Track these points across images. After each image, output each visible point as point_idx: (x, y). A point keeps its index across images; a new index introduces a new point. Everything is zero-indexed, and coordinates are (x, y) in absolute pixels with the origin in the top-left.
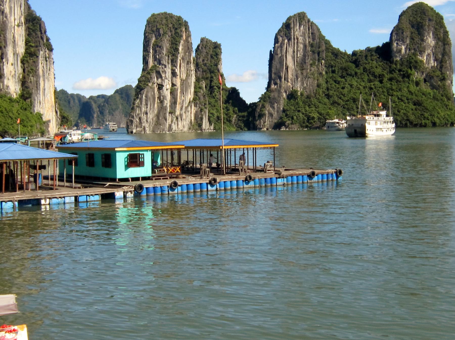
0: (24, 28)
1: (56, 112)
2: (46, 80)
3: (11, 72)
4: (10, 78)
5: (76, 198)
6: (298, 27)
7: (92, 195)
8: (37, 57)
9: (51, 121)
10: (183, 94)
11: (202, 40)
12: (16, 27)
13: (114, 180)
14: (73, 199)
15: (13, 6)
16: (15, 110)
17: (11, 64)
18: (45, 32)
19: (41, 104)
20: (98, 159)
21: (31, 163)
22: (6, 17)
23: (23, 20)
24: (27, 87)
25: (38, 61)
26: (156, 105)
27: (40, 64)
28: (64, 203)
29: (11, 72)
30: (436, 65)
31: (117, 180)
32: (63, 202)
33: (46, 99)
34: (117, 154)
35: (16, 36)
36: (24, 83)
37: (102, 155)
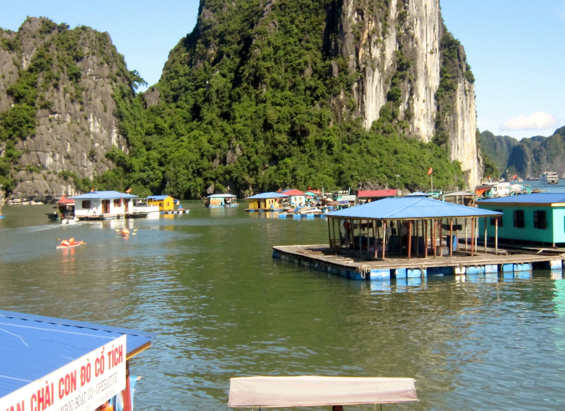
0: (438, 55)
1: (478, 160)
2: (466, 119)
3: (422, 110)
4: (422, 118)
5: (499, 266)
7: (520, 264)
8: (455, 90)
9: (472, 171)
12: (429, 55)
13: (550, 245)
14: (495, 268)
15: (424, 29)
16: (426, 157)
17: (422, 101)
18: (465, 59)
19: (460, 150)
20: (529, 218)
21: (444, 222)
22: (417, 43)
23: (437, 45)
24: (442, 129)
27: (458, 99)
28: (484, 273)
31: (554, 245)
32: (482, 271)
33: (466, 143)
34: (555, 211)
35: (429, 66)
36: (438, 124)
37: (534, 212)
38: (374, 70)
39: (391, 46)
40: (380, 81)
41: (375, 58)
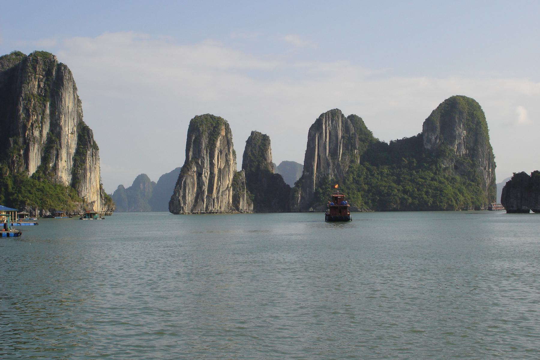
2: (92, 172)
4: (64, 171)
6: (330, 122)
10: (220, 180)
11: (253, 133)
12: (69, 135)
17: (64, 162)
23: (75, 129)
25: (85, 159)
26: (195, 190)
27: (88, 160)
29: (64, 166)
30: (468, 152)
38: (34, 143)
39: (46, 130)
40: (38, 150)
41: (36, 137)
